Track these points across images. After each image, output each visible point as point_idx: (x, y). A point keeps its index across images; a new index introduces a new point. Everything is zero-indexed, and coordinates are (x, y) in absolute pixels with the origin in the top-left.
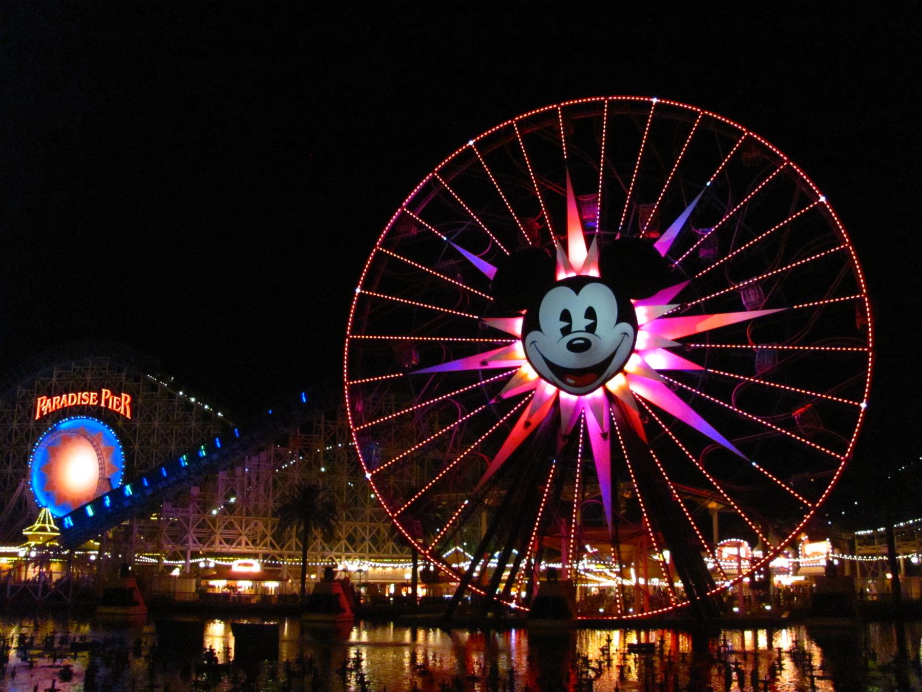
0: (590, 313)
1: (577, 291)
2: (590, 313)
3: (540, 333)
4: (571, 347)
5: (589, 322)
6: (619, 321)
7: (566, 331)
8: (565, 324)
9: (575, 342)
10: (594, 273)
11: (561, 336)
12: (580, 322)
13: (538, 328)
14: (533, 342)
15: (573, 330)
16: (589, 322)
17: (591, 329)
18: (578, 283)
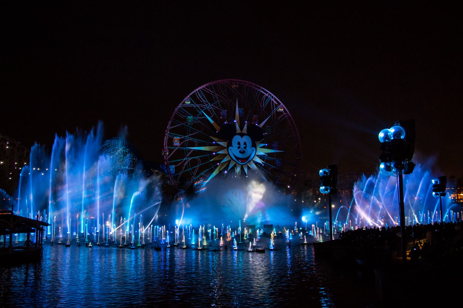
0: (245, 144)
1: (242, 137)
2: (245, 144)
3: (232, 147)
4: (240, 152)
5: (245, 146)
6: (252, 147)
7: (239, 148)
8: (239, 146)
9: (241, 151)
10: (246, 132)
11: (238, 149)
12: (242, 146)
13: (232, 146)
14: (231, 150)
15: (241, 147)
16: (245, 146)
17: (245, 148)
18: (242, 135)
